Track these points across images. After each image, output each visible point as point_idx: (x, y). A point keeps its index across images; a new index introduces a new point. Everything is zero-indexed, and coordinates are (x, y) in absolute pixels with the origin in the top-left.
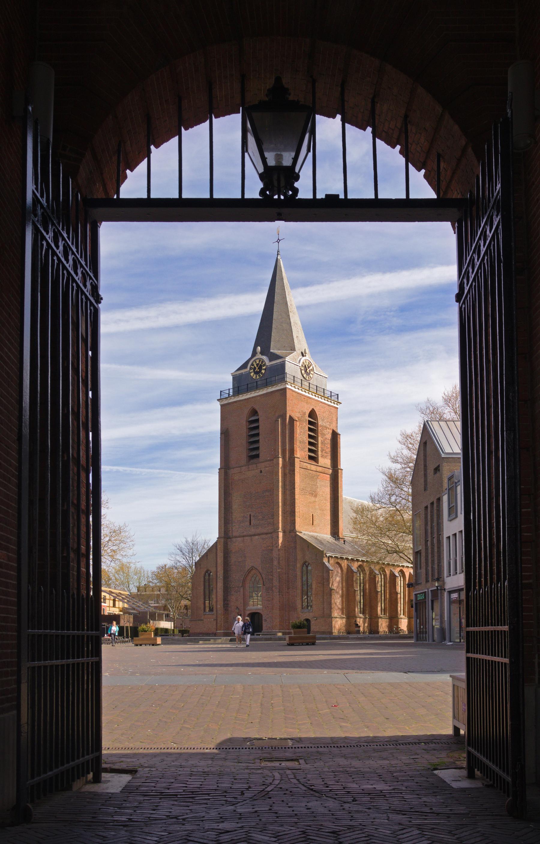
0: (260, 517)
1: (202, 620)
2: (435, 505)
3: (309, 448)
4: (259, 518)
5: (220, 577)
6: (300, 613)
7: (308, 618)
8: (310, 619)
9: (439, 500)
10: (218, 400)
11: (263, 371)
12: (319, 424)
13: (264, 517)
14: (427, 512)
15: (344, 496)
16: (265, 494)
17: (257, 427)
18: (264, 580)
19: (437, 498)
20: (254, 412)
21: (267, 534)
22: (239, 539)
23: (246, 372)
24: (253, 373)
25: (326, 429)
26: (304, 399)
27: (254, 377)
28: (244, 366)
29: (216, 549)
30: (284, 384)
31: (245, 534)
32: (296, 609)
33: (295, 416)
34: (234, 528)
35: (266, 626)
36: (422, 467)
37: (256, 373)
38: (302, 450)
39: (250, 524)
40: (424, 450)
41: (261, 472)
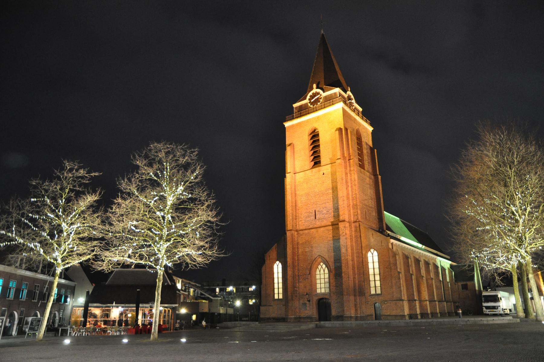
0: (325, 212)
1: (271, 306)
4: (324, 212)
5: (289, 266)
16: (328, 192)
32: (364, 294)
35: (335, 311)
39: (316, 218)
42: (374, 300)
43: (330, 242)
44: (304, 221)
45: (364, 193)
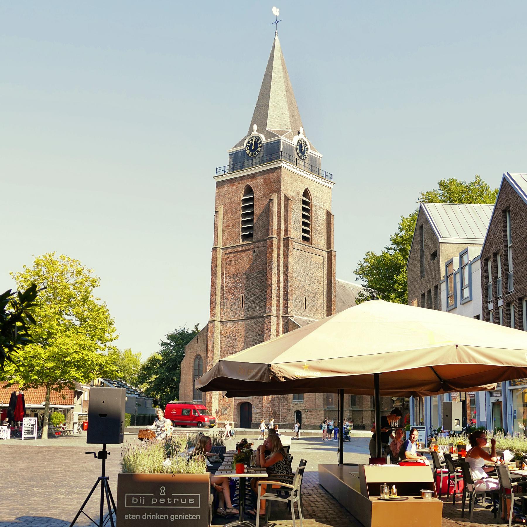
0: (253, 300)
2: (433, 293)
3: (303, 229)
4: (251, 300)
7: (299, 409)
8: (301, 410)
9: (437, 288)
10: (213, 177)
11: (259, 149)
12: (314, 204)
13: (256, 300)
14: (424, 300)
15: (337, 279)
17: (252, 206)
19: (434, 286)
20: (249, 190)
21: (258, 317)
24: (249, 150)
25: (320, 210)
26: (299, 178)
27: (249, 155)
28: (241, 144)
29: (207, 332)
30: (279, 162)
33: (291, 194)
35: (256, 417)
36: (419, 251)
37: (251, 151)
38: (296, 230)
40: (420, 234)
42: (296, 407)
43: (256, 337)
44: (230, 309)
45: (306, 276)
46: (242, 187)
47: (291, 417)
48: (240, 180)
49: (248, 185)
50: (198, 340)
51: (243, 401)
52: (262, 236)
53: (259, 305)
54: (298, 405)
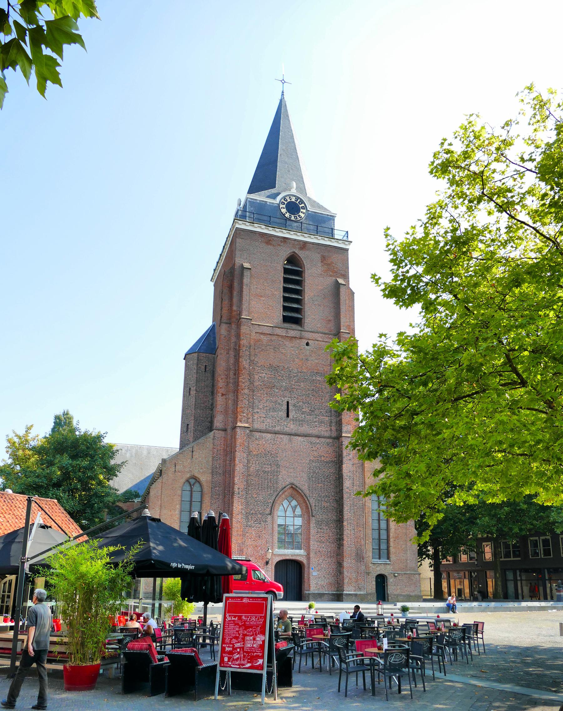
0: (306, 410)
4: (304, 410)
6: (371, 565)
18: (313, 508)
21: (318, 437)
22: (266, 434)
23: (273, 203)
31: (277, 429)
34: (256, 417)
35: (317, 584)
39: (288, 416)
41: (307, 344)
43: (314, 464)
46: (285, 252)
47: (371, 586)
48: (281, 242)
49: (294, 252)
50: (194, 453)
51: (287, 558)
52: (319, 326)
53: (317, 419)
54: (382, 567)
